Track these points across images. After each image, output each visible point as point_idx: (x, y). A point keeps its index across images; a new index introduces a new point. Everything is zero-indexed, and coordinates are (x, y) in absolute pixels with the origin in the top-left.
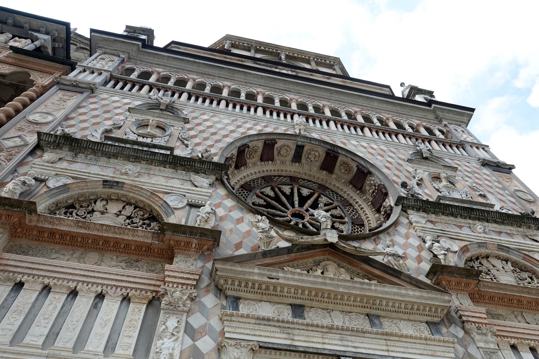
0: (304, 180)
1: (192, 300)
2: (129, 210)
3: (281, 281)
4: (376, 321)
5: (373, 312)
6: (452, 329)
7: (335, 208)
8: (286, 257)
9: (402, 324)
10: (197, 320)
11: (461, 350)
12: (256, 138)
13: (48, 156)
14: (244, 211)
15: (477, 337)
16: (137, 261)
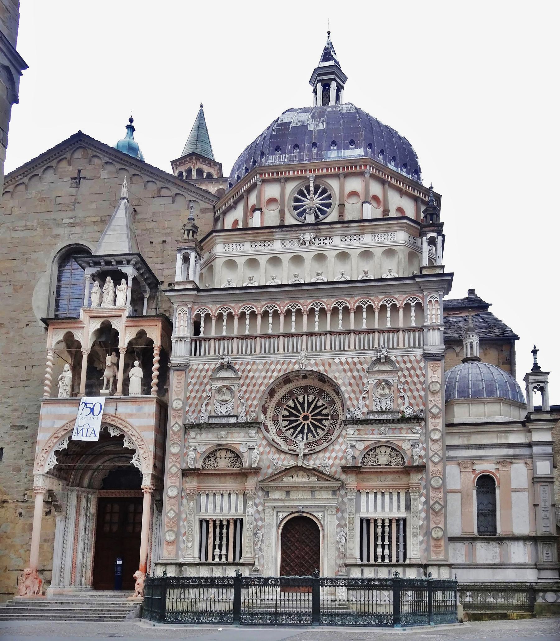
0: (311, 387)
1: (255, 494)
2: (229, 453)
3: (281, 485)
4: (313, 493)
5: (313, 490)
6: (341, 492)
7: (326, 408)
8: (283, 473)
9: (323, 492)
10: (257, 501)
11: (340, 499)
12: (277, 381)
13: (192, 434)
14: (271, 446)
15: (349, 494)
16: (237, 478)
